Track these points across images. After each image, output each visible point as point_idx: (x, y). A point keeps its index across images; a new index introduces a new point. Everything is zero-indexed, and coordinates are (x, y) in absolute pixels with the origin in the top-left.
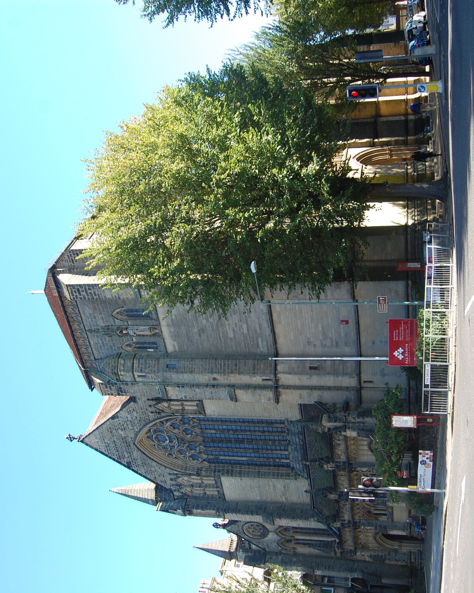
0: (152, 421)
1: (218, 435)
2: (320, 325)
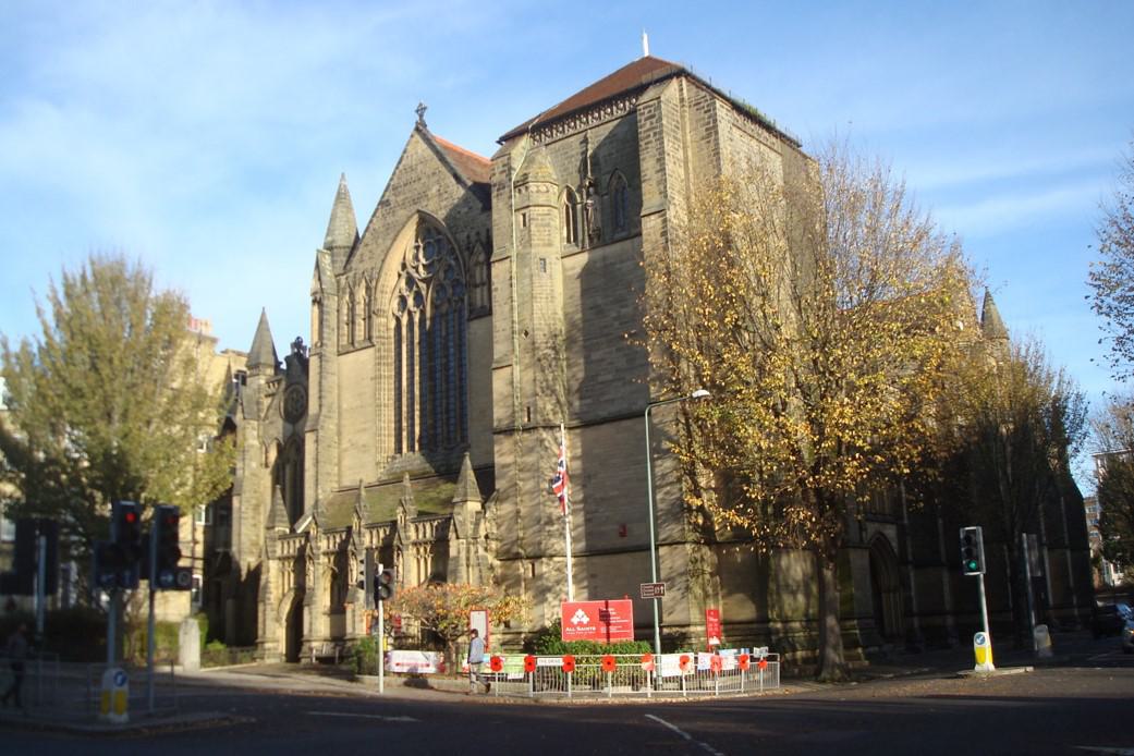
0: (456, 239)
1: (438, 340)
2: (616, 493)
